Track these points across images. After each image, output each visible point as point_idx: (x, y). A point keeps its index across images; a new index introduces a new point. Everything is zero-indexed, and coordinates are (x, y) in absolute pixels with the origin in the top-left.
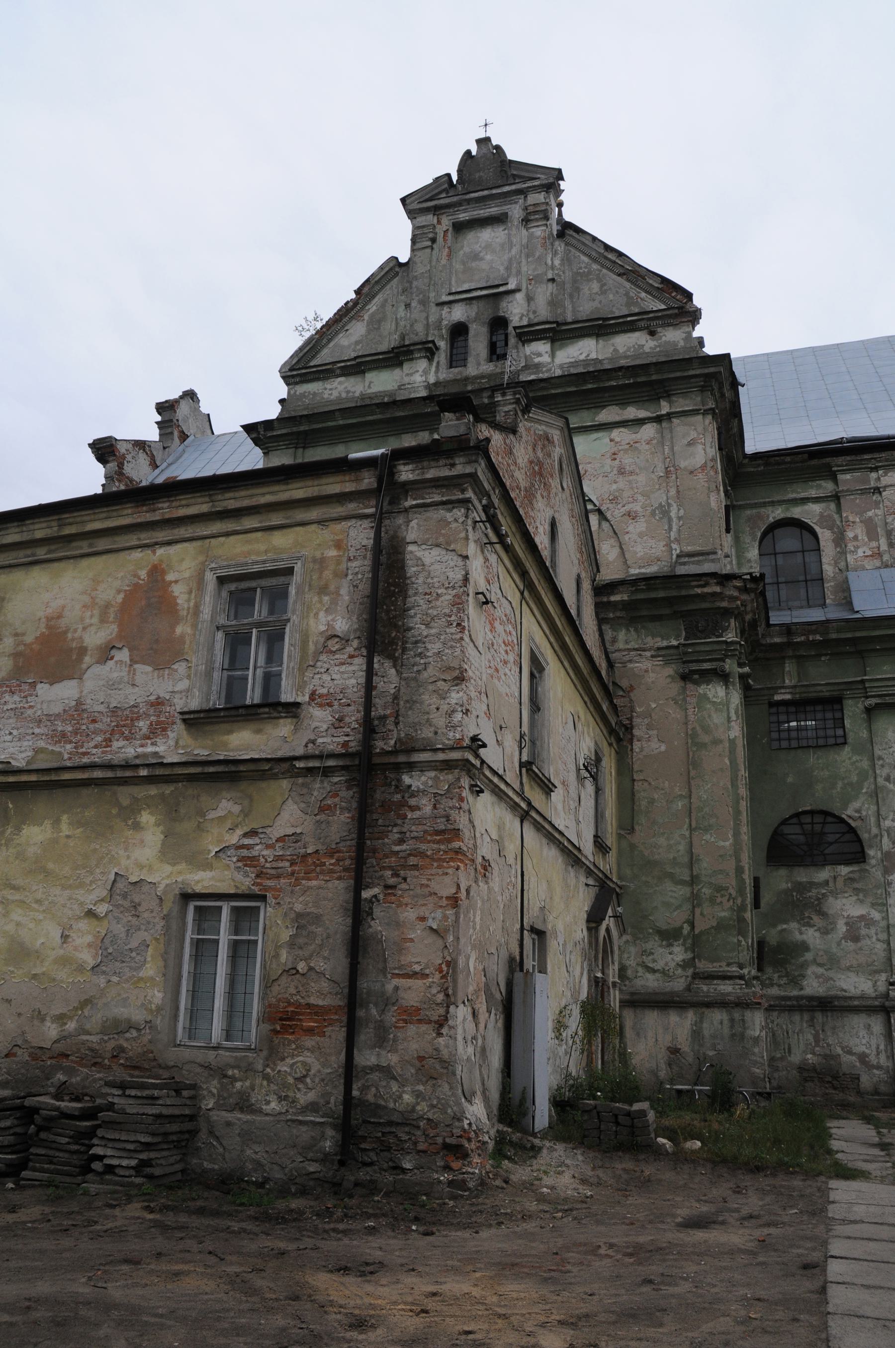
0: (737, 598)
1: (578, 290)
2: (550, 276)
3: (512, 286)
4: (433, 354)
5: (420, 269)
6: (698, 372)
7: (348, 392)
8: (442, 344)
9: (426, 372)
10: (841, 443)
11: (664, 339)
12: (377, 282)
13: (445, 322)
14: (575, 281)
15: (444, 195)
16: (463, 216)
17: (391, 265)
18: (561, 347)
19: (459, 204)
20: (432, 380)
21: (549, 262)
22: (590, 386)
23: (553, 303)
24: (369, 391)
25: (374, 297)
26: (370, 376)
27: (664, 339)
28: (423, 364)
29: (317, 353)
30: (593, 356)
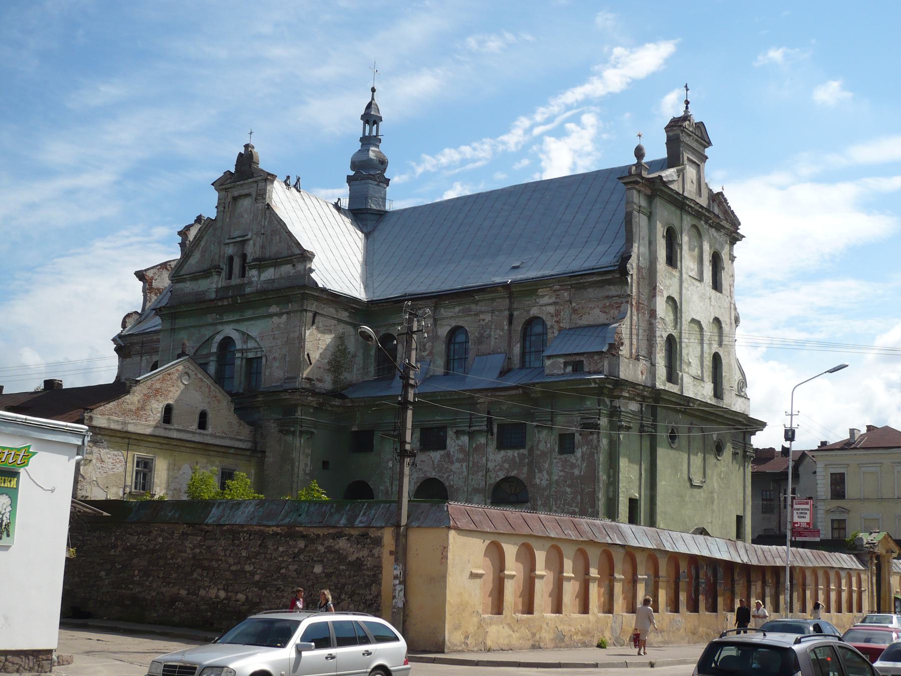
0: (298, 399)
1: (272, 240)
2: (262, 232)
3: (249, 237)
4: (220, 272)
5: (219, 224)
6: (298, 292)
7: (193, 289)
8: (225, 267)
9: (217, 282)
10: (405, 296)
11: (297, 269)
12: (204, 230)
13: (226, 255)
14: (271, 235)
15: (229, 181)
16: (236, 194)
17: (208, 221)
18: (263, 271)
19: (234, 187)
20: (220, 286)
21: (263, 224)
22: (264, 297)
23: (263, 247)
24: (200, 290)
25: (203, 238)
26: (200, 282)
27: (297, 269)
28: (215, 278)
29: (183, 267)
30: (273, 278)
